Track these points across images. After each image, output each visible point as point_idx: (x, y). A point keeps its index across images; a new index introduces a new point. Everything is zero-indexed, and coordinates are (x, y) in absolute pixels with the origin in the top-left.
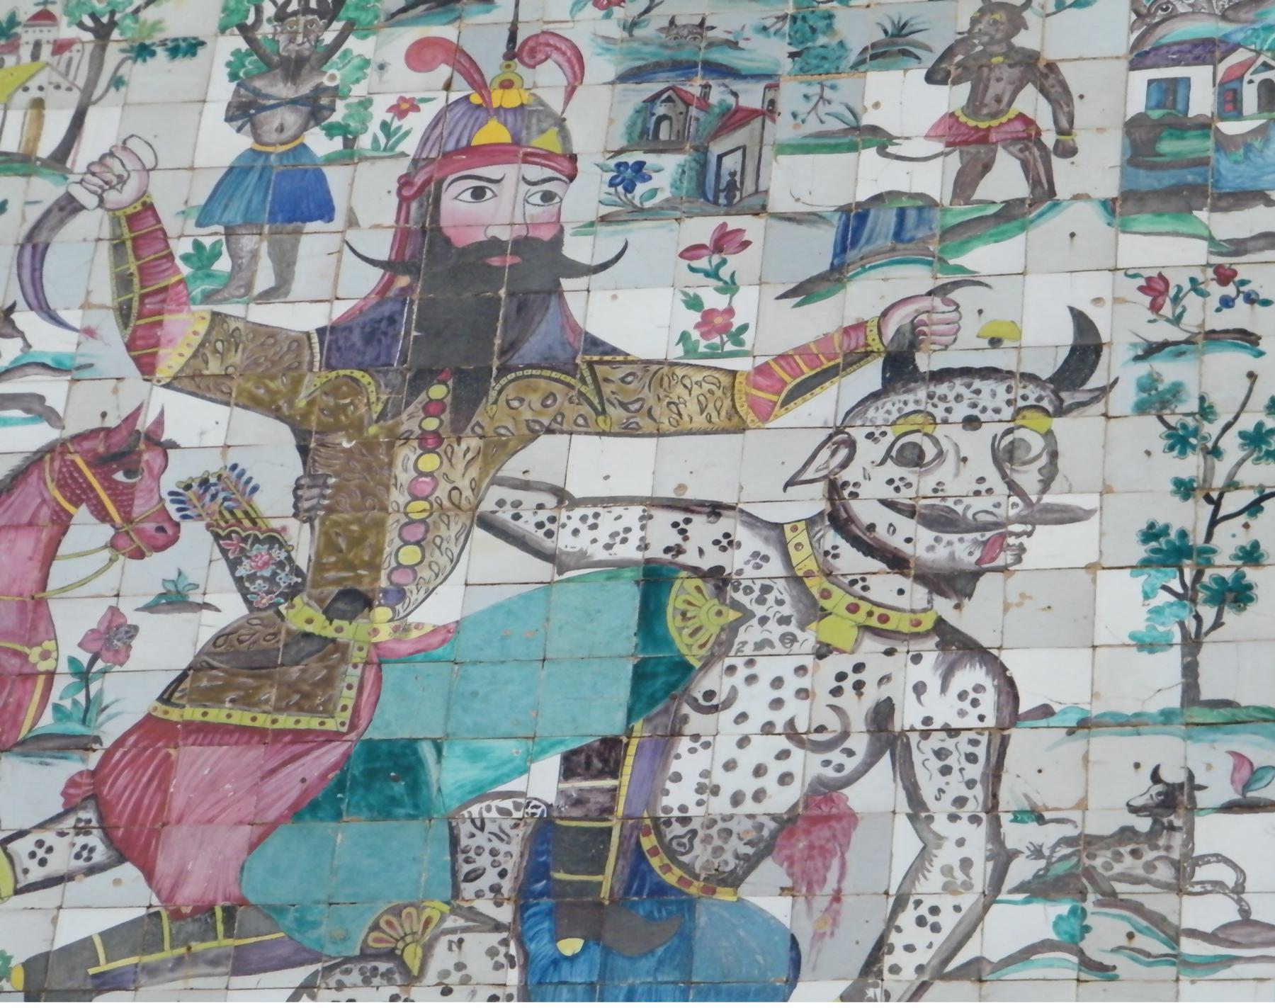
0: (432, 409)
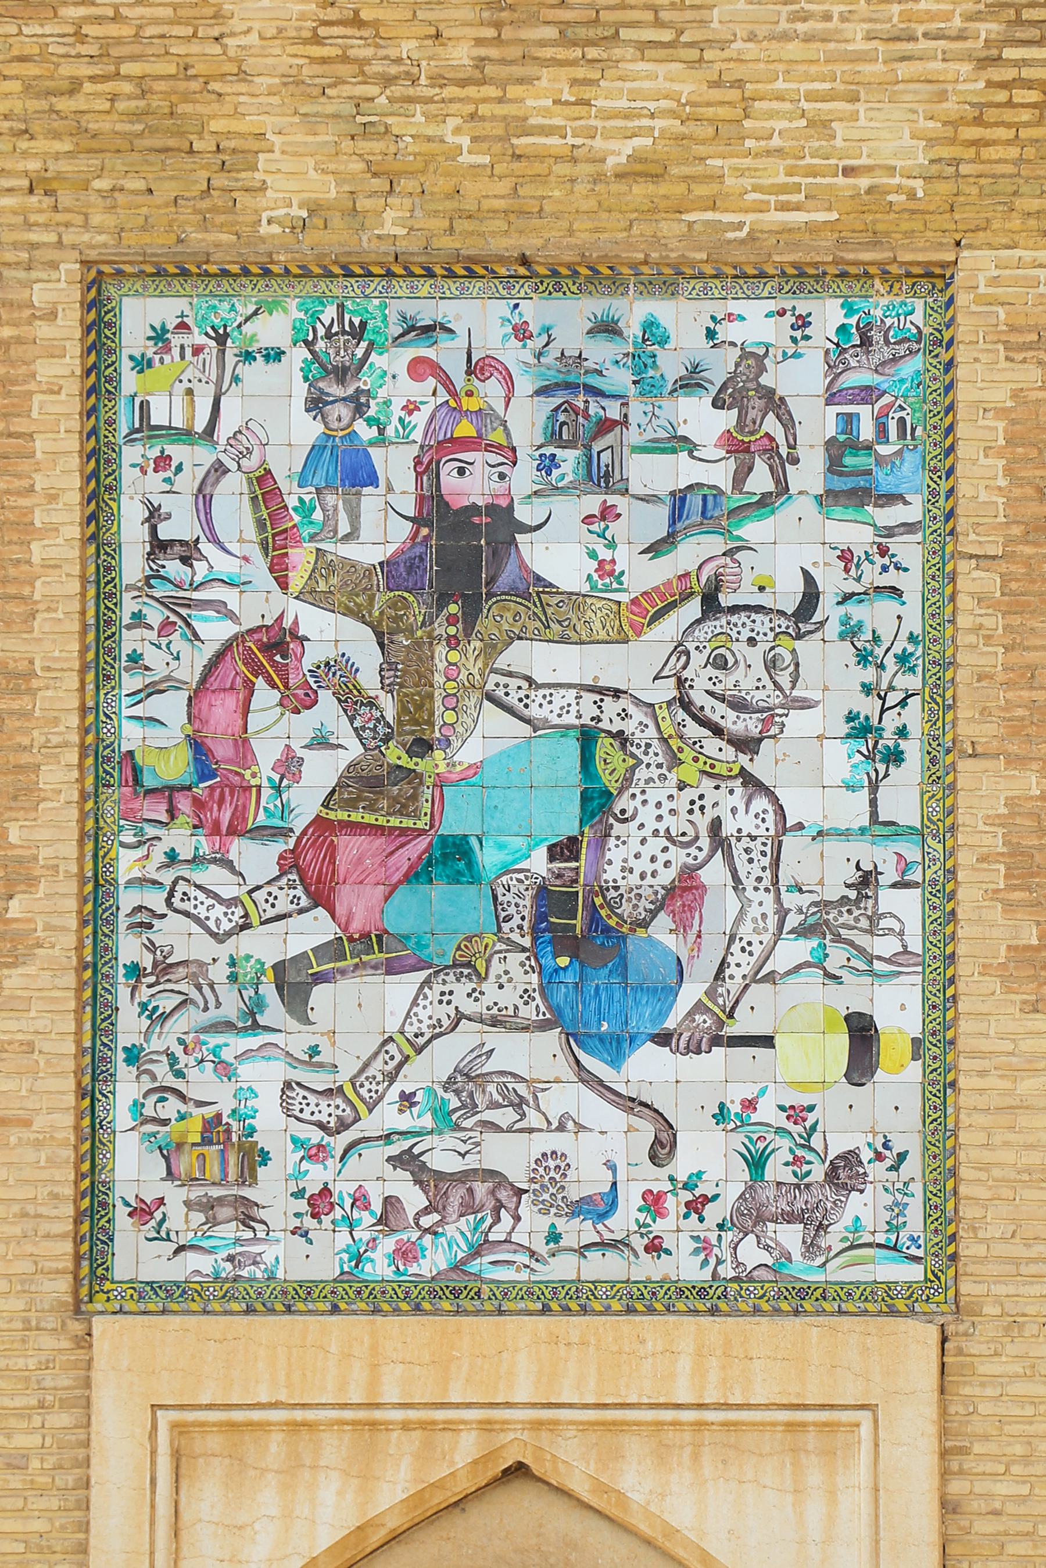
0: (452, 620)
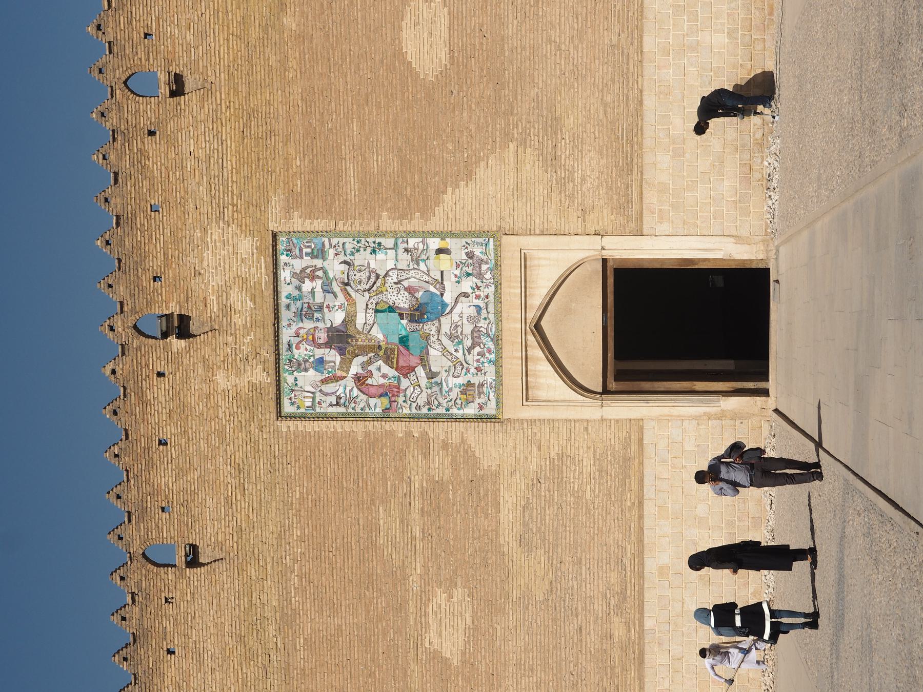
0: (352, 341)
